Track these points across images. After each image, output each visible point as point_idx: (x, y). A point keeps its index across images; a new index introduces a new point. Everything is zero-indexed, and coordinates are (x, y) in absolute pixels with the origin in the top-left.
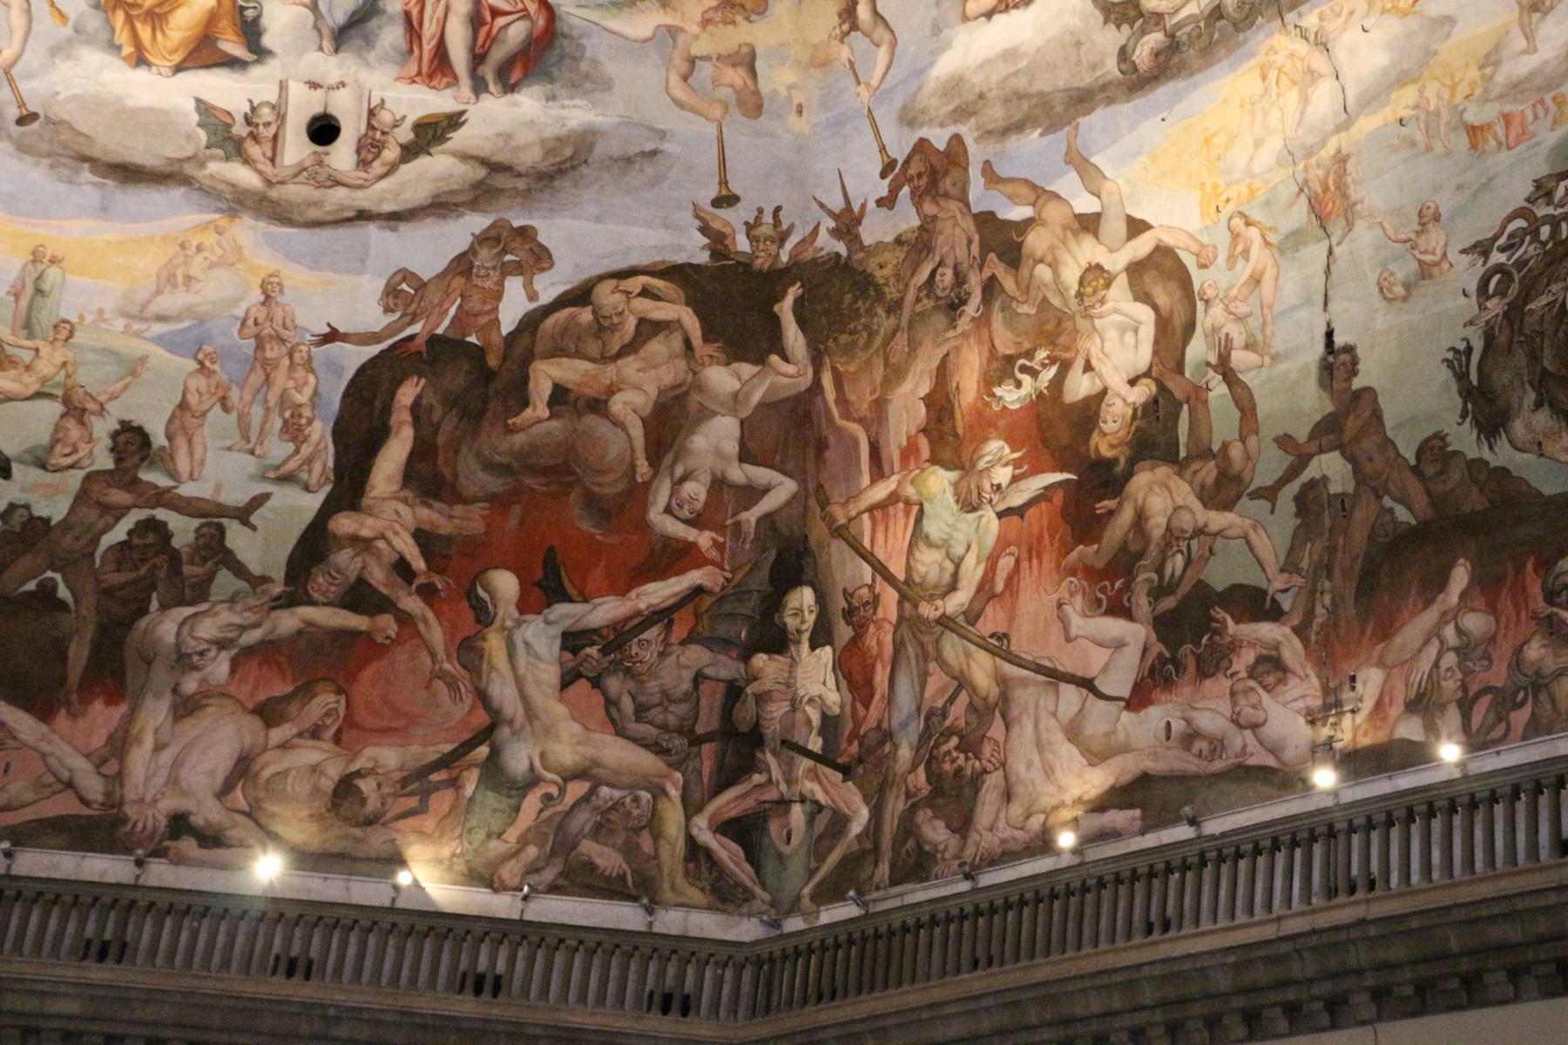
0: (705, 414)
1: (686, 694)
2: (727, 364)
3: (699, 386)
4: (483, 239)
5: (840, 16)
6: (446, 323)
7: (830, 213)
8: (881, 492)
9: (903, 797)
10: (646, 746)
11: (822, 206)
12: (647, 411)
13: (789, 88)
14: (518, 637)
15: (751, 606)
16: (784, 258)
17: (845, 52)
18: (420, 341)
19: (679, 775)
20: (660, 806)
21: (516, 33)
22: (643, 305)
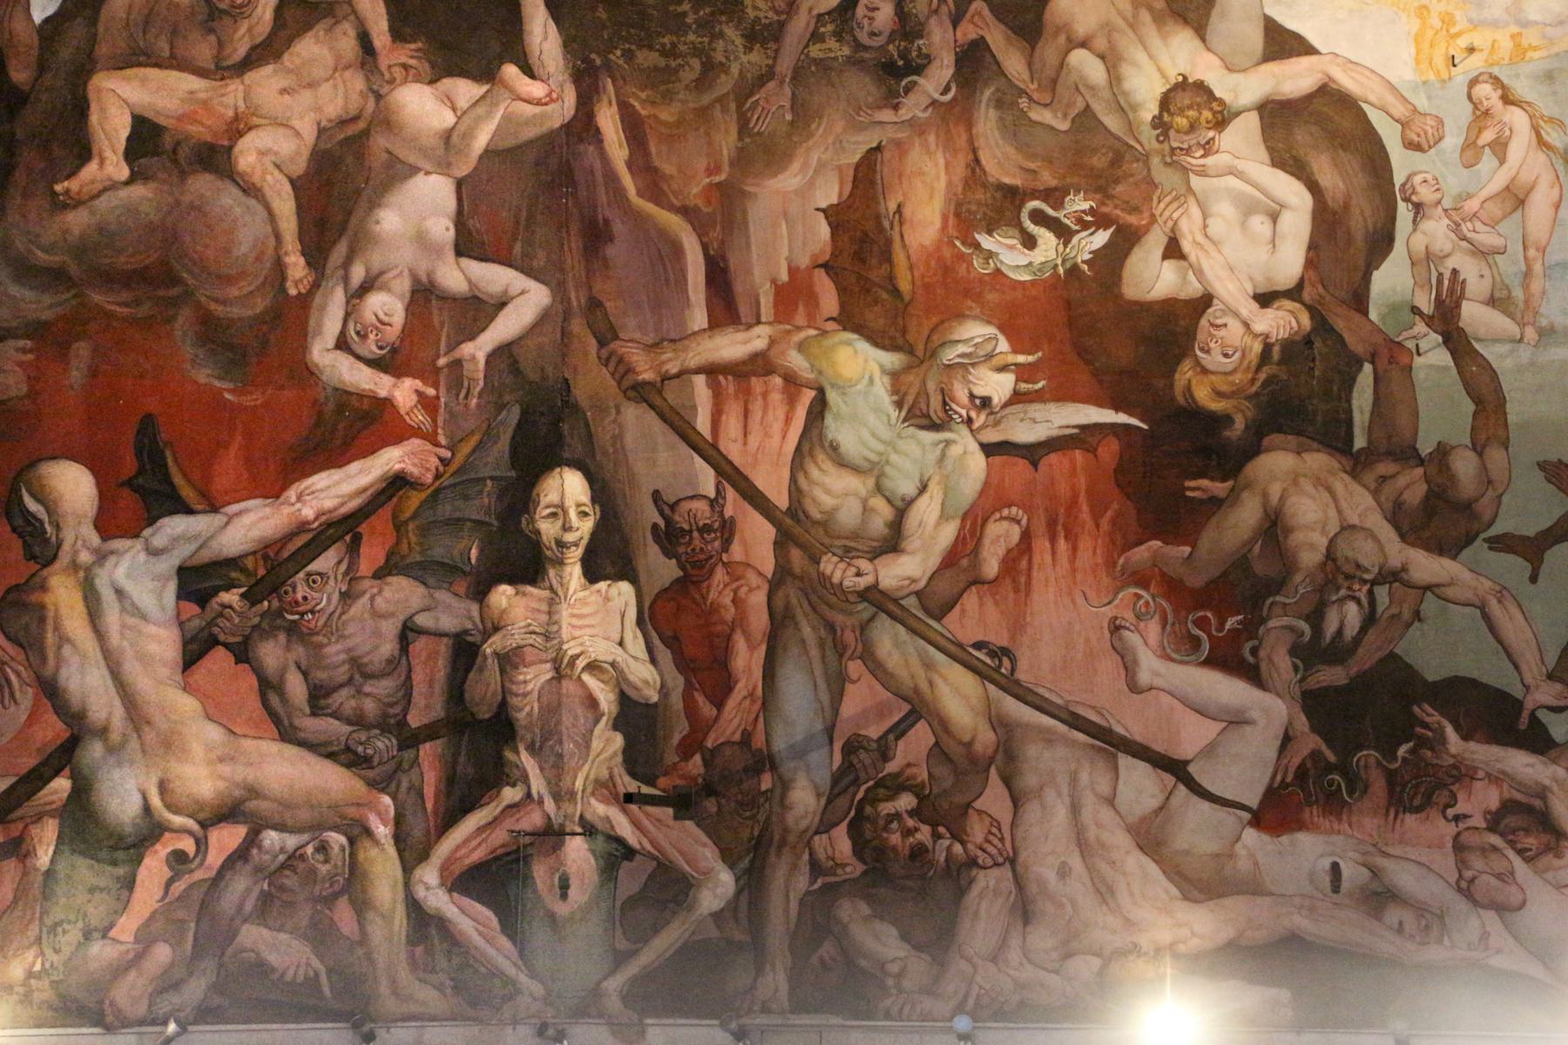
0: (398, 172)
1: (389, 661)
2: (432, 82)
3: (385, 120)
8: (732, 346)
9: (805, 868)
10: (330, 756)
12: (299, 167)
14: (102, 583)
15: (483, 504)
19: (387, 800)
20: (361, 856)
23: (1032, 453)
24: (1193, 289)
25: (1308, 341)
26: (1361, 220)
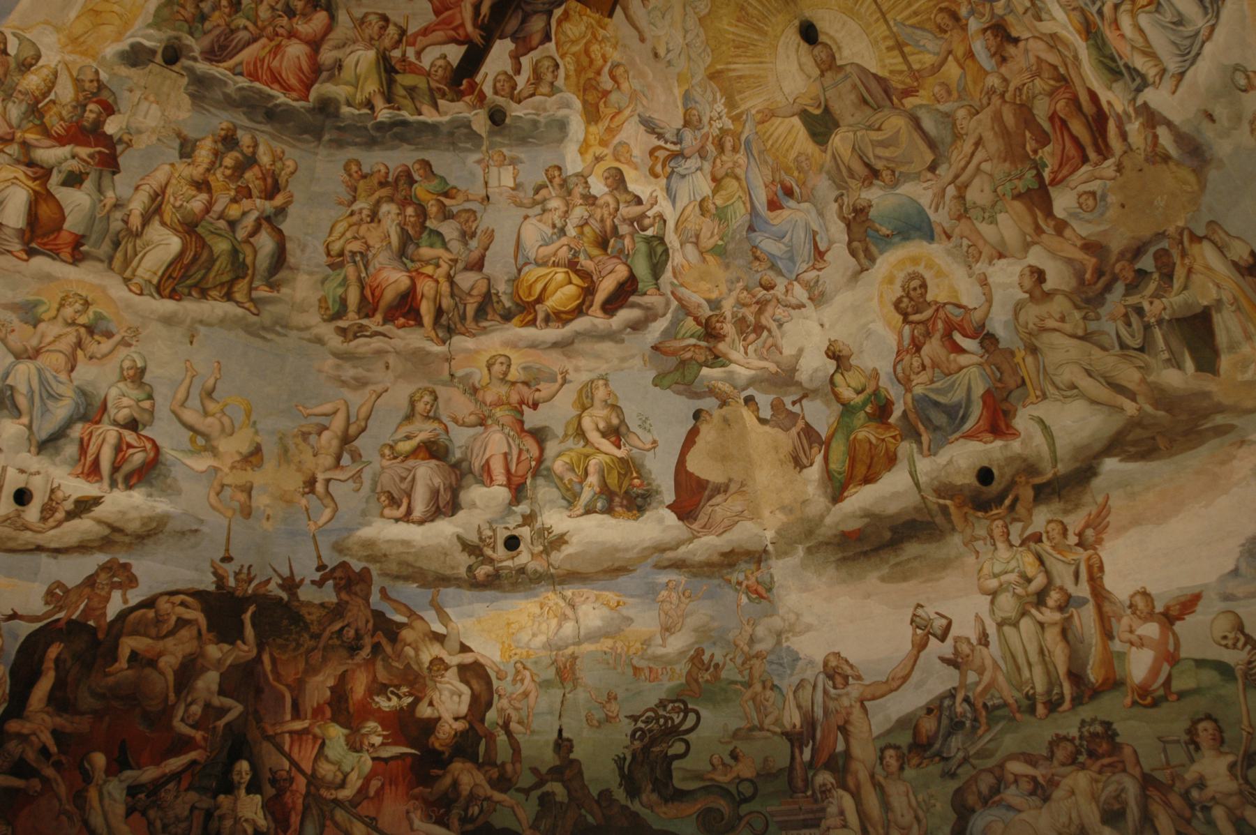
0: (204, 670)
4: (104, 568)
5: (304, 483)
6: (78, 613)
7: (280, 576)
8: (298, 725)
11: (275, 570)
12: (176, 667)
13: (267, 506)
16: (250, 591)
17: (304, 502)
18: (62, 623)
21: (138, 458)
22: (181, 610)
23: (386, 760)
24: (436, 715)
25: (467, 731)
26: (484, 698)
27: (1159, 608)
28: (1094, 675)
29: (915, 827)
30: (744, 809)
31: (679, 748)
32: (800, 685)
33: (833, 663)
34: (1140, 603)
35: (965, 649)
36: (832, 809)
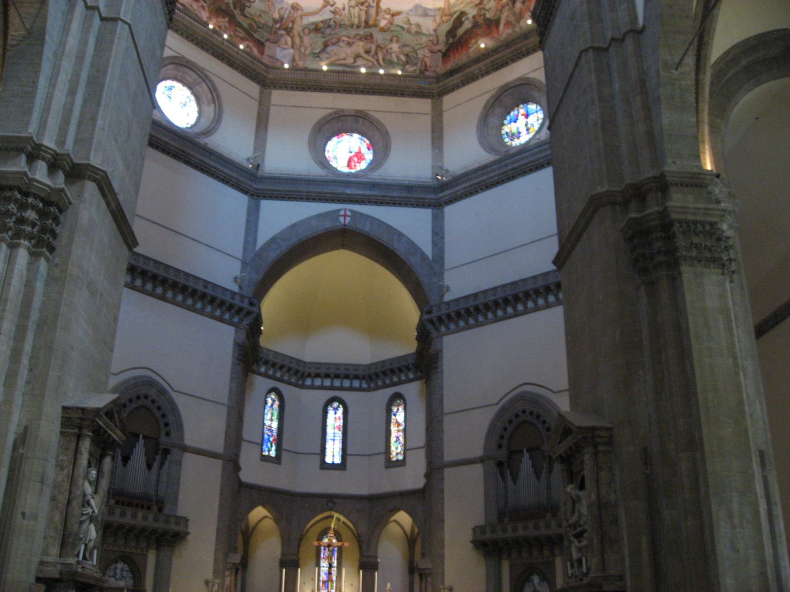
27: (392, 12)
28: (371, 22)
29: (310, 48)
30: (259, 30)
31: (248, 5)
32: (282, 8)
33: (295, 5)
34: (387, 10)
35: (338, 10)
36: (283, 40)
